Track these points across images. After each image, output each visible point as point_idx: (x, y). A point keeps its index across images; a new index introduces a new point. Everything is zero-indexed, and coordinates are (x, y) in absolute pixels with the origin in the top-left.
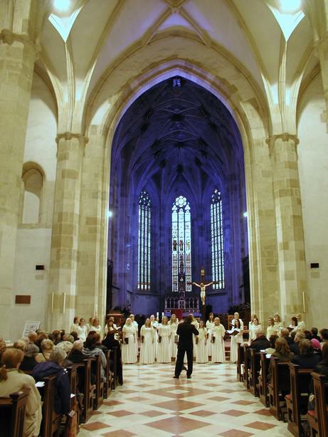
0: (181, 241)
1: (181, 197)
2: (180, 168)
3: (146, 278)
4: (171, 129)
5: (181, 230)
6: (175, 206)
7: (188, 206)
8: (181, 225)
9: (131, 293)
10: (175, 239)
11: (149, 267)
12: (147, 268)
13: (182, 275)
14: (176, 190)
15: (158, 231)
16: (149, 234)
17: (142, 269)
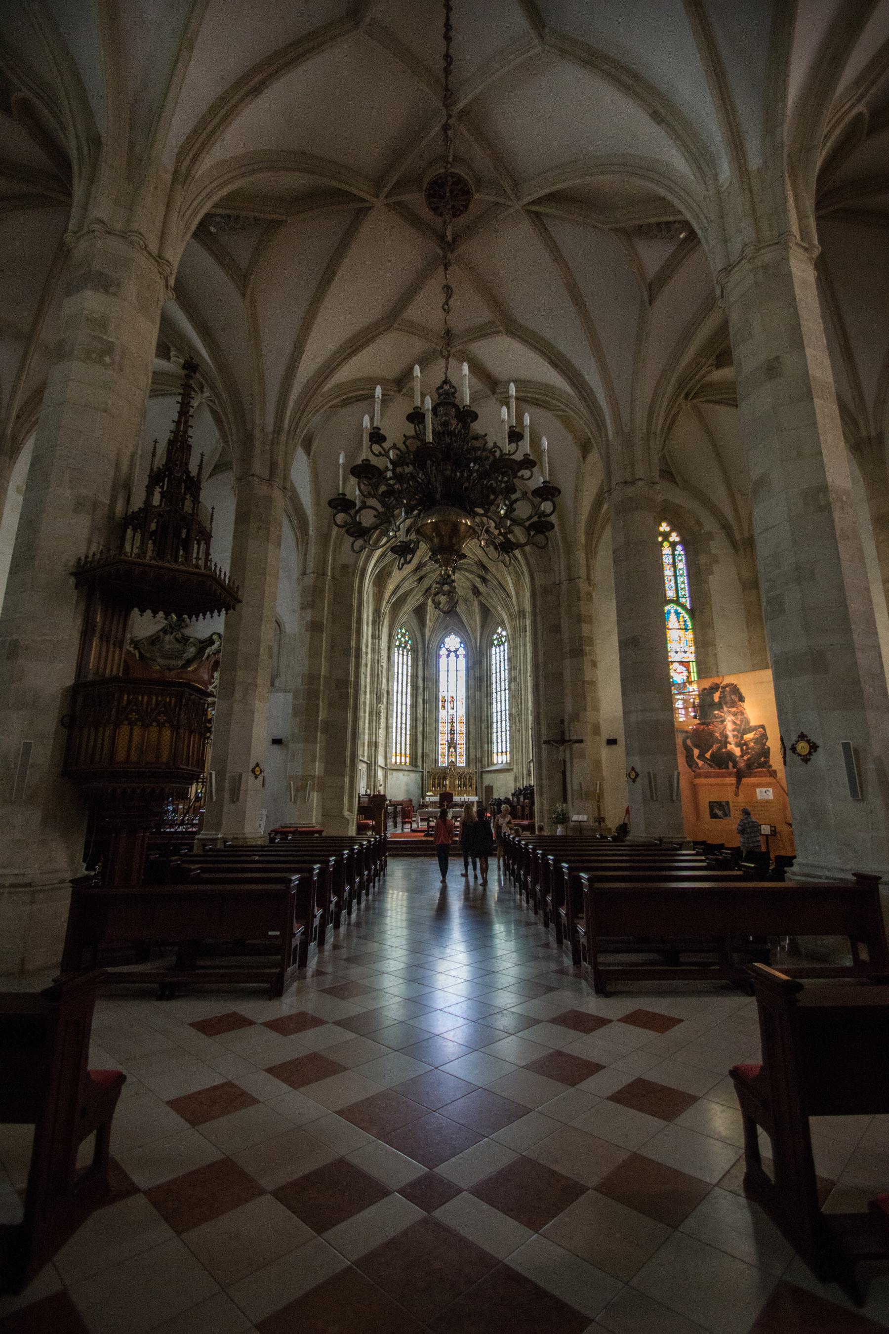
0: (452, 697)
1: (452, 636)
6: (443, 649)
11: (408, 733)
13: (452, 744)
14: (446, 628)
16: (409, 687)
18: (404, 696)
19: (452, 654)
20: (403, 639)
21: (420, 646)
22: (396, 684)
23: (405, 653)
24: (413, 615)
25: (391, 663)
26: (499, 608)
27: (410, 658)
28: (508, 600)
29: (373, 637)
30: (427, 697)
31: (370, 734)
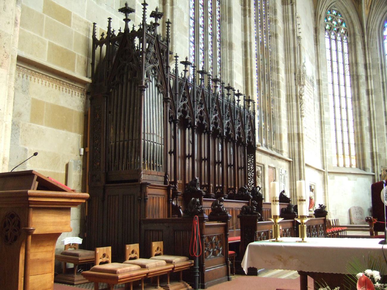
3: (346, 146)
9: (320, 171)
15: (361, 70)
16: (348, 78)
17: (339, 133)
20: (334, 23)
21: (357, 28)
22: (329, 74)
23: (339, 39)
25: (321, 48)
27: (345, 45)
30: (371, 85)
31: (290, 124)
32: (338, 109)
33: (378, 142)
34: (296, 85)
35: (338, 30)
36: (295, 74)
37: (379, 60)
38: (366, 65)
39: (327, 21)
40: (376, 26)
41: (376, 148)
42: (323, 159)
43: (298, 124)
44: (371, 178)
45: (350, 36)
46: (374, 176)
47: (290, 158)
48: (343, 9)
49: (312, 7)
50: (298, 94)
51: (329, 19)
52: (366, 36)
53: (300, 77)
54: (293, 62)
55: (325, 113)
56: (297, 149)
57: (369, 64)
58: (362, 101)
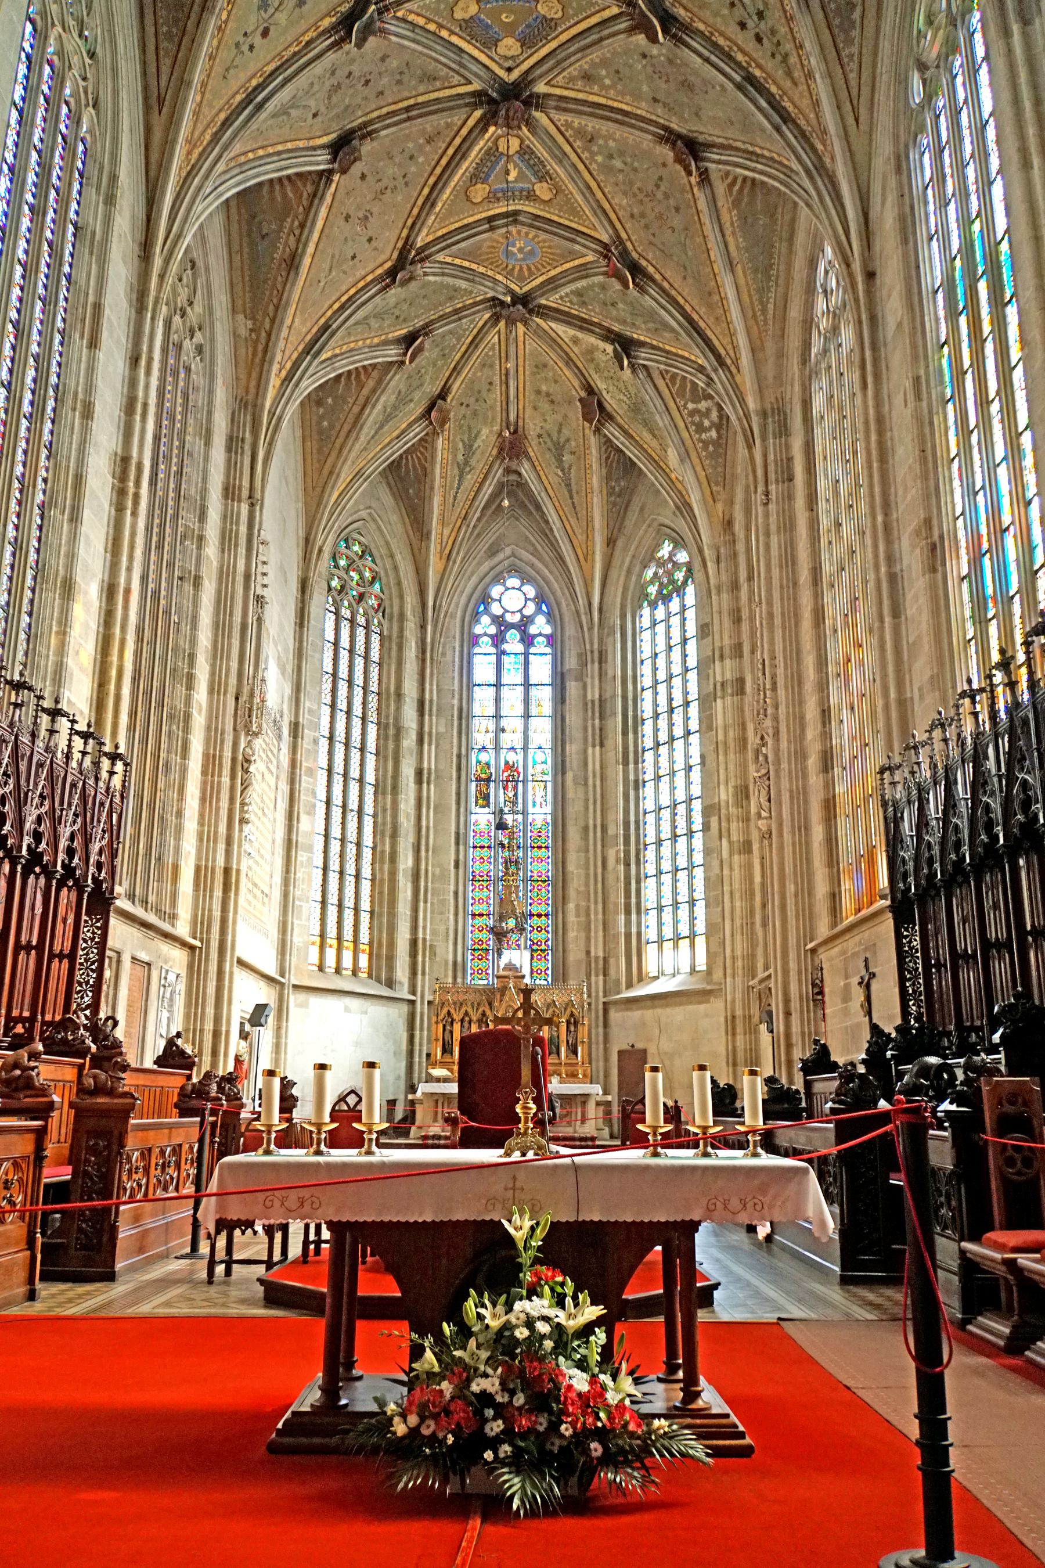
2: (512, 446)
4: (479, 192)
5: (513, 724)
6: (485, 620)
7: (541, 620)
8: (512, 699)
10: (484, 757)
11: (366, 872)
12: (358, 877)
16: (372, 730)
18: (355, 755)
19: (513, 635)
21: (411, 600)
23: (361, 620)
24: (386, 498)
25: (311, 636)
26: (672, 456)
27: (375, 640)
28: (720, 377)
29: (229, 492)
30: (429, 762)
32: (337, 813)
33: (432, 912)
34: (235, 729)
35: (361, 597)
36: (237, 699)
37: (457, 696)
38: (421, 703)
39: (337, 566)
40: (457, 605)
41: (424, 928)
42: (283, 948)
43: (229, 842)
44: (405, 1008)
45: (391, 619)
46: (412, 1003)
47: (195, 938)
48: (381, 542)
49: (301, 524)
50: (240, 757)
51: (342, 563)
52: (429, 628)
53: (250, 710)
54: (234, 664)
55: (304, 817)
56: (217, 914)
57: (431, 701)
58: (402, 796)
